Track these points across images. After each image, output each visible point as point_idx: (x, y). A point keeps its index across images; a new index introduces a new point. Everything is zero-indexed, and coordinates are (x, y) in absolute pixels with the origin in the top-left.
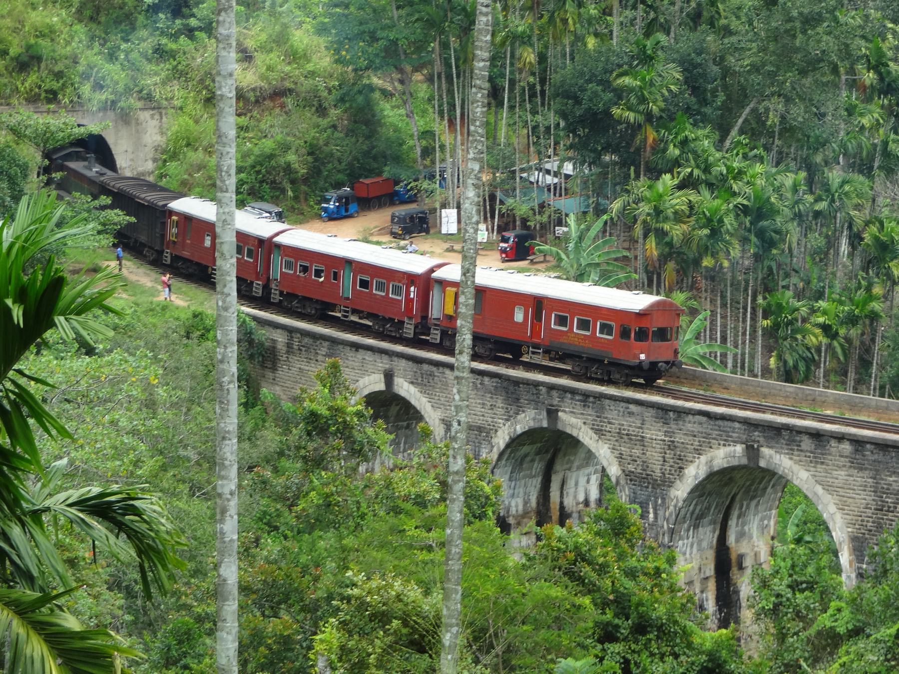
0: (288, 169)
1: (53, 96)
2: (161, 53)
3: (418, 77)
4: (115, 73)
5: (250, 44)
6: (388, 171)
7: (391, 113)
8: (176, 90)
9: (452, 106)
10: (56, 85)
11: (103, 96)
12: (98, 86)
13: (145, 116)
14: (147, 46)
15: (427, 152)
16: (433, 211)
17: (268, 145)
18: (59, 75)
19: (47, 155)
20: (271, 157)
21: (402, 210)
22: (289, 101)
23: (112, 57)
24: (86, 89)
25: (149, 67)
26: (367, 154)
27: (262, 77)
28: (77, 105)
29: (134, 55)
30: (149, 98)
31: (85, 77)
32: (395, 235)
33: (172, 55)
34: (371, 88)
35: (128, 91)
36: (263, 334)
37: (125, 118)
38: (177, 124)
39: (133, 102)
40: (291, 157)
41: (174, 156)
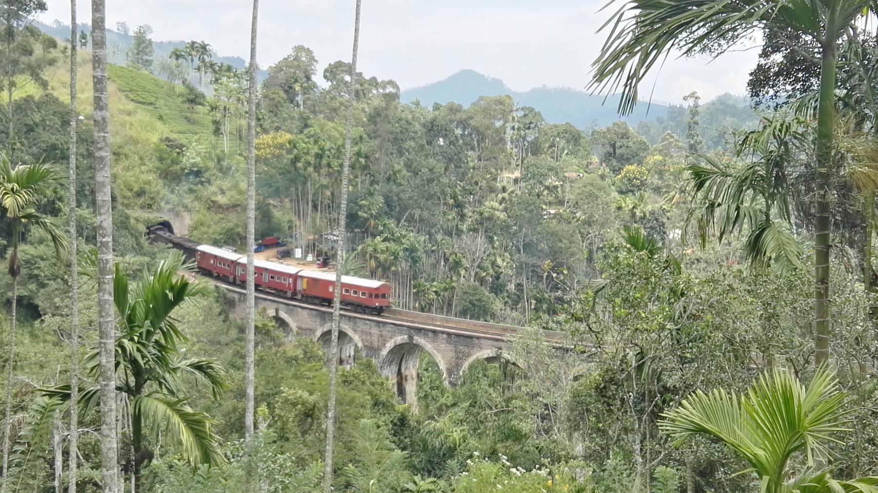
0: (238, 234)
1: (150, 206)
2: (191, 191)
3: (287, 200)
4: (173, 198)
5: (224, 188)
6: (276, 235)
7: (277, 213)
8: (196, 204)
9: (299, 210)
10: (151, 202)
11: (169, 206)
12: (167, 203)
13: (185, 214)
14: (186, 188)
15: (290, 228)
16: (292, 249)
17: (231, 225)
18: (152, 199)
19: (148, 228)
20: (232, 229)
21: (281, 249)
22: (239, 209)
23: (172, 192)
24: (163, 204)
25: (186, 196)
26: (268, 228)
27: (229, 200)
28: (159, 210)
29: (181, 191)
30: (186, 207)
31: (162, 199)
32: (278, 258)
33: (195, 191)
34: (269, 204)
35: (178, 205)
36: (230, 295)
37: (177, 214)
38: (196, 217)
39: (180, 208)
40: (240, 230)
41: (196, 228)
